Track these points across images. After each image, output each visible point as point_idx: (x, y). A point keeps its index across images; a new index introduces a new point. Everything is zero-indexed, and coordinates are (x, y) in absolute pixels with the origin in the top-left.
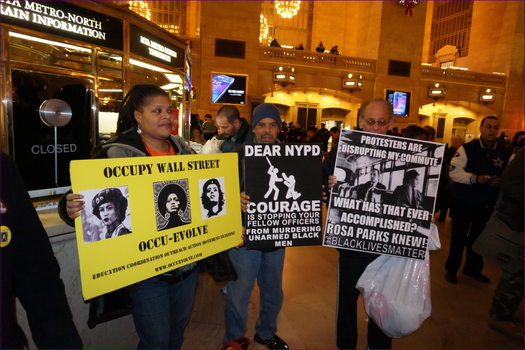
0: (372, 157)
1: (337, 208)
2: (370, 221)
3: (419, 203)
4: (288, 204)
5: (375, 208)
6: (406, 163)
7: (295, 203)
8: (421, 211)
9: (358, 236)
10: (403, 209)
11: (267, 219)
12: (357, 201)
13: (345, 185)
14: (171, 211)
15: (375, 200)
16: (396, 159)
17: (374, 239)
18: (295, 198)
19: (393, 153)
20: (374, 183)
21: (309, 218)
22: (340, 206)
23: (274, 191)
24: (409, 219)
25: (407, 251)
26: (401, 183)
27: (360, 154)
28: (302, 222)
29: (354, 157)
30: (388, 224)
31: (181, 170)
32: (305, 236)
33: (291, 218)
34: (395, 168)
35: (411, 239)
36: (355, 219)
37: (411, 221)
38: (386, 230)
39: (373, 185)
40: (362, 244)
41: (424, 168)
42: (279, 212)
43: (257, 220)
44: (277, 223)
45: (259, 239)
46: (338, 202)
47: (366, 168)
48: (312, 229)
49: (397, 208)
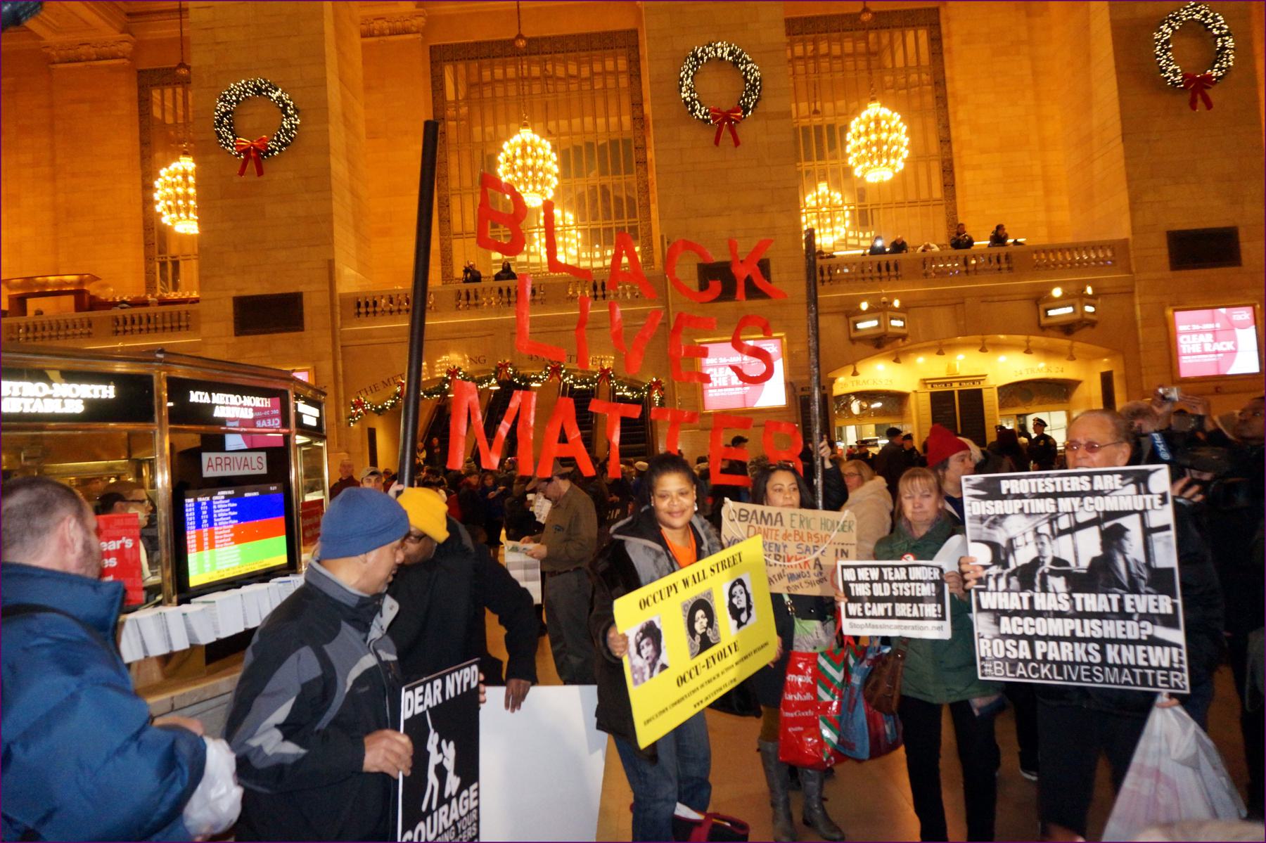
0: (1030, 514)
1: (989, 610)
9: (1039, 657)
12: (1022, 594)
13: (994, 570)
16: (1076, 509)
17: (1071, 659)
19: (1068, 500)
22: (993, 607)
29: (997, 521)
36: (1027, 625)
40: (1051, 670)
46: (988, 600)
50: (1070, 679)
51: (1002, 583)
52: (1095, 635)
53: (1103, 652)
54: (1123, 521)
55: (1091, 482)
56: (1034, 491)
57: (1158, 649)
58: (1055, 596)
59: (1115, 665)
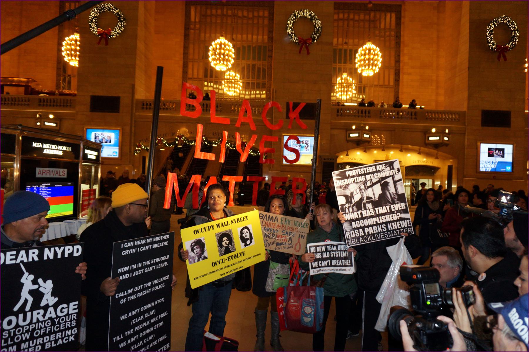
1: (348, 221)
2: (371, 221)
3: (396, 200)
8: (399, 204)
9: (367, 234)
10: (388, 207)
13: (347, 205)
22: (349, 219)
24: (394, 212)
25: (400, 232)
26: (381, 192)
29: (346, 187)
34: (373, 184)
35: (400, 223)
36: (361, 223)
38: (383, 223)
40: (371, 238)
46: (347, 217)
49: (384, 207)
50: (378, 239)
54: (387, 180)
55: (376, 168)
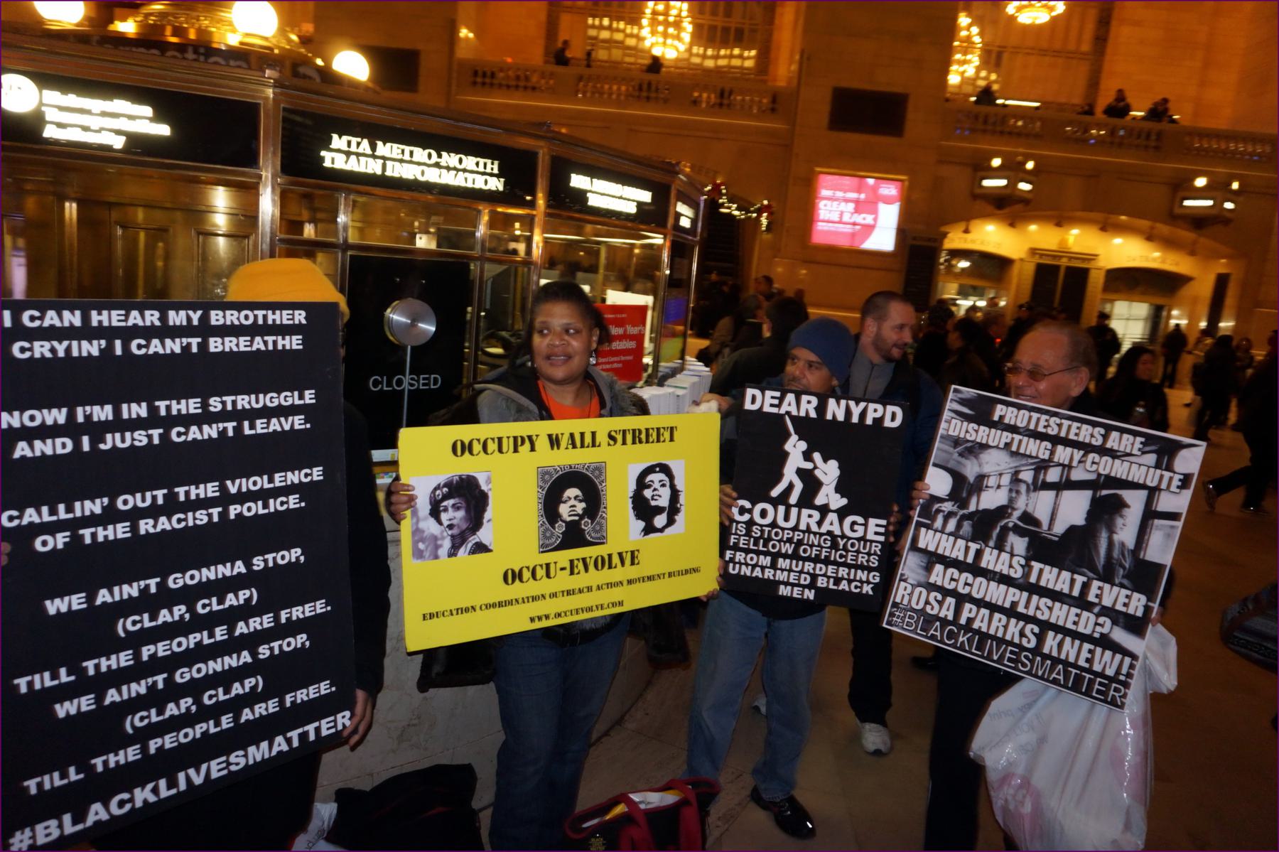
0: (1016, 454)
1: (924, 552)
2: (996, 593)
4: (816, 515)
5: (1011, 566)
6: (1099, 475)
7: (832, 517)
8: (1125, 592)
9: (963, 621)
10: (1080, 579)
11: (770, 539)
12: (970, 544)
13: (948, 506)
14: (569, 519)
15: (1012, 548)
16: (1075, 463)
17: (1000, 635)
18: (833, 506)
19: (1069, 450)
20: (1014, 509)
21: (858, 552)
22: (931, 548)
23: (791, 486)
24: (1093, 604)
26: (1079, 519)
27: (991, 443)
28: (841, 556)
29: (976, 449)
30: (1038, 608)
31: (594, 445)
32: (844, 586)
33: (819, 545)
34: (1067, 484)
37: (1096, 610)
39: (1010, 515)
41: (1143, 494)
42: (795, 529)
43: (751, 537)
44: (788, 548)
45: (748, 574)
46: (928, 540)
47: (1001, 475)
48: (862, 575)
49: (1066, 575)
50: (989, 657)
51: (952, 525)
52: (1039, 615)
53: (1041, 638)
54: (1127, 495)
55: (1105, 437)
56: (1032, 427)
57: (1108, 654)
58: (1008, 558)
59: (1048, 657)
